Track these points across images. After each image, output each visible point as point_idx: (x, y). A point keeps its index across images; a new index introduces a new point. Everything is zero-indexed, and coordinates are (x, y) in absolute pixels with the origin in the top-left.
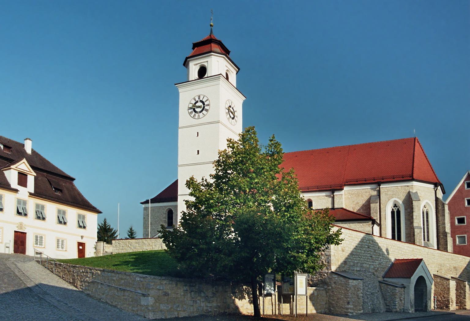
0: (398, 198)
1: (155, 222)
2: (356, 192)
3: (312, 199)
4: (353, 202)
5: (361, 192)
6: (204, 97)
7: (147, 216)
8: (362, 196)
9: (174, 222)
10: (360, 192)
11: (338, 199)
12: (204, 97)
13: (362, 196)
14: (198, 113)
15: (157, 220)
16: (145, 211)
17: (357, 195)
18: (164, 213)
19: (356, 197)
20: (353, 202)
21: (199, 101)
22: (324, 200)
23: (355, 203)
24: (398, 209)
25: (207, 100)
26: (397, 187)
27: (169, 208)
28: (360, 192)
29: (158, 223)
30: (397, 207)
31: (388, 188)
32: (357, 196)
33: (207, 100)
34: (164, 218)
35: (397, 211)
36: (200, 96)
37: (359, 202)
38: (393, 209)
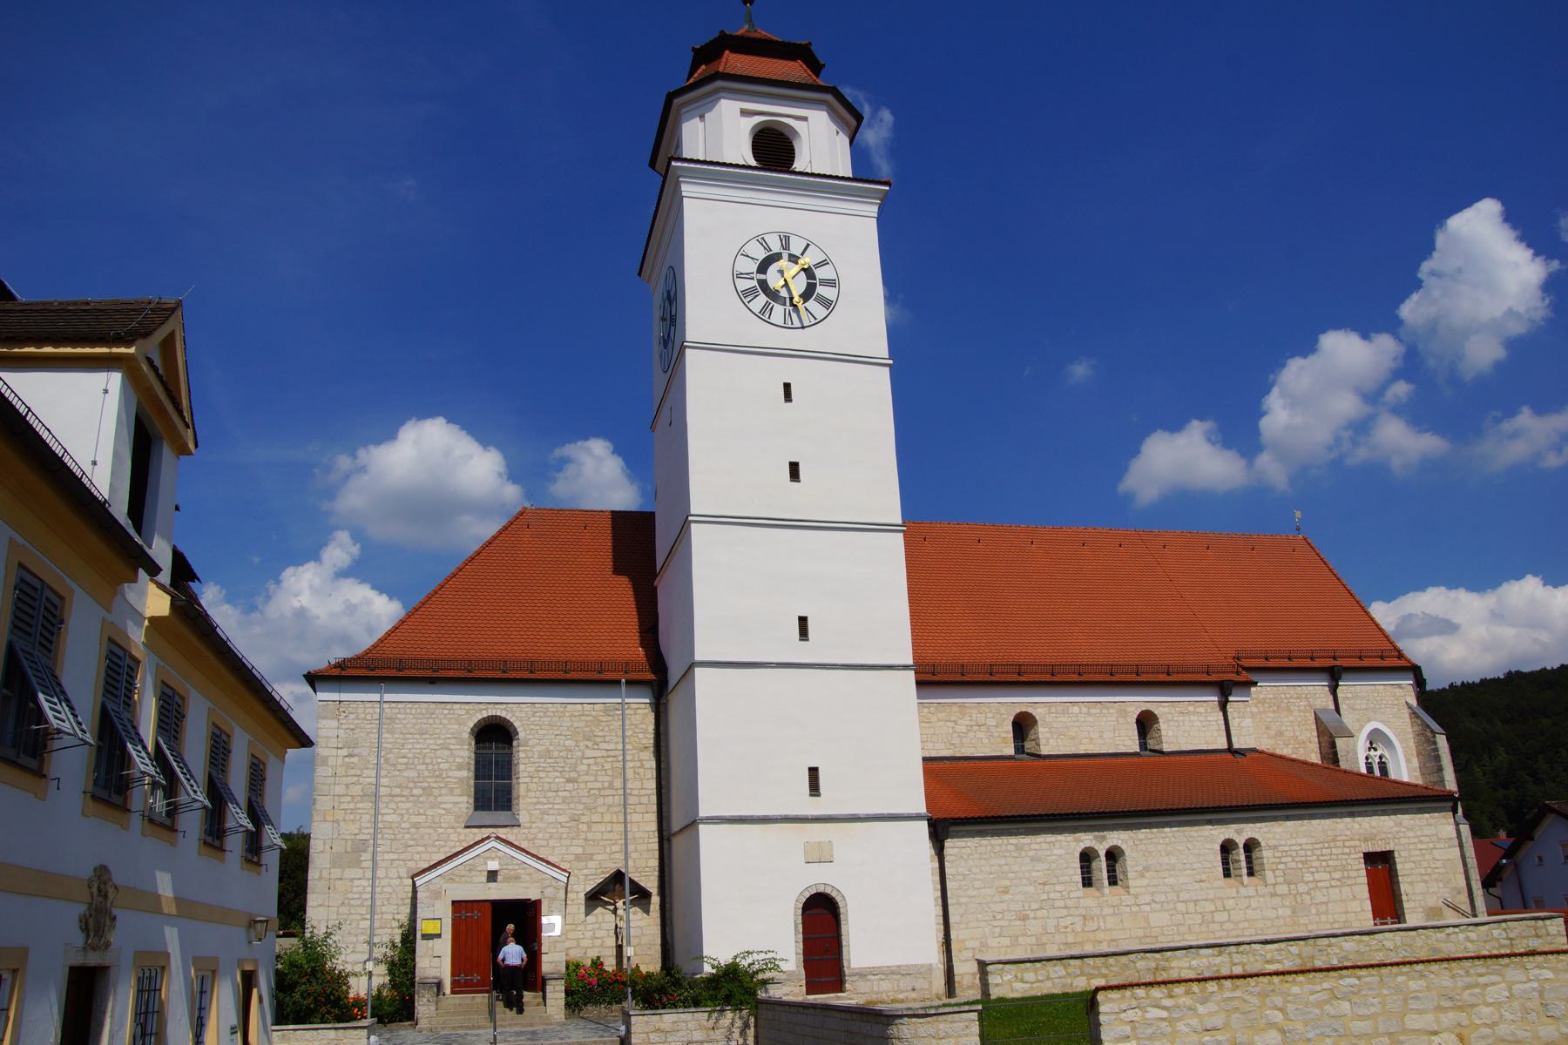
0: (1382, 722)
1: (399, 787)
2: (1271, 696)
3: (1156, 712)
4: (1268, 728)
5: (1285, 694)
6: (808, 245)
7: (345, 752)
8: (1289, 710)
9: (528, 790)
10: (1283, 696)
11: (1236, 715)
12: (808, 245)
13: (1289, 710)
14: (785, 305)
15: (413, 774)
16: (334, 723)
17: (1275, 704)
18: (460, 741)
19: (1274, 712)
20: (1268, 728)
21: (785, 256)
22: (1196, 718)
23: (1272, 732)
24: (1381, 757)
25: (824, 263)
26: (1373, 687)
27: (492, 712)
28: (1283, 696)
29: (417, 792)
30: (1375, 749)
31: (1353, 688)
32: (1275, 708)
33: (824, 263)
34: (460, 767)
35: (1379, 763)
36: (787, 239)
37: (1283, 728)
38: (1367, 758)
